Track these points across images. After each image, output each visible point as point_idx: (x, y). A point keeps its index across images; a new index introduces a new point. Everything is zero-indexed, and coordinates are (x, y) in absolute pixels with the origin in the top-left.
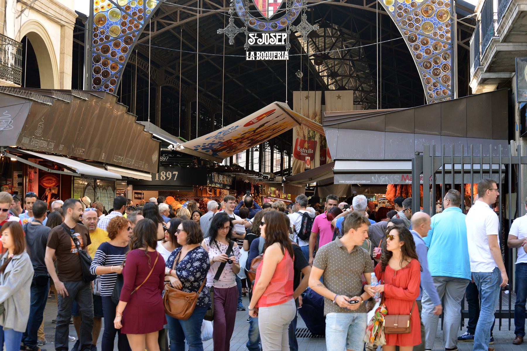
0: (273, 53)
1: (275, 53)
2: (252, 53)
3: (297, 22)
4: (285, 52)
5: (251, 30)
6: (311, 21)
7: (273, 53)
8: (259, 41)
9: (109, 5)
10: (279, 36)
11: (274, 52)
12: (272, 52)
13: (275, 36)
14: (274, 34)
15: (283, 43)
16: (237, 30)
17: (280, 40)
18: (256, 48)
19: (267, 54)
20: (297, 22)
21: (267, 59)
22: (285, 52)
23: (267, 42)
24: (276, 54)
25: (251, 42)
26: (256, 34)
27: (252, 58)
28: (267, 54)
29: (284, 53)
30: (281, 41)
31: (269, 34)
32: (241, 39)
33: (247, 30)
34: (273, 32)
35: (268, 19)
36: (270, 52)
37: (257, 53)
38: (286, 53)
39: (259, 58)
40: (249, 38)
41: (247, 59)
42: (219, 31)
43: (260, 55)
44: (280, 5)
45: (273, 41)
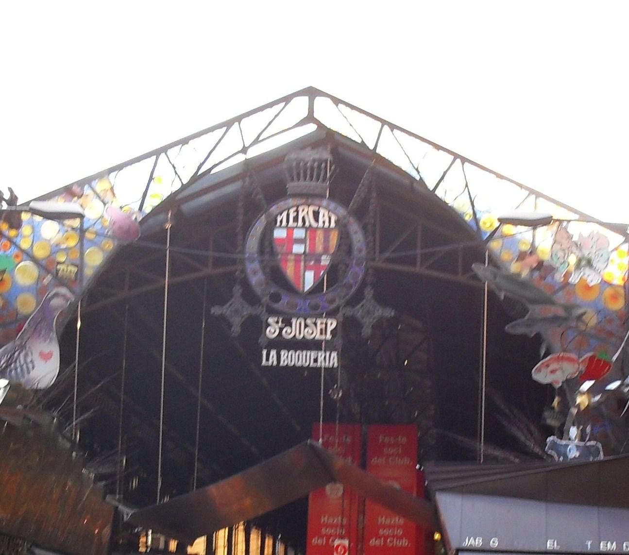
1: (313, 354)
3: (356, 299)
5: (272, 312)
6: (381, 299)
9: (17, 256)
13: (315, 324)
15: (329, 336)
16: (247, 310)
18: (280, 344)
20: (356, 299)
21: (299, 364)
23: (300, 333)
25: (272, 332)
31: (305, 320)
32: (256, 326)
33: (265, 311)
34: (311, 316)
38: (334, 354)
40: (268, 325)
41: (264, 362)
42: (216, 310)
43: (287, 357)
44: (325, 269)
45: (310, 332)
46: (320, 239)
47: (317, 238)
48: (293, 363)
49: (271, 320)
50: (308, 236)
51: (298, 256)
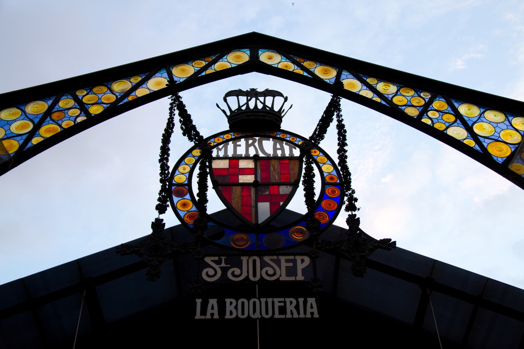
0: (273, 302)
1: (277, 302)
2: (213, 302)
4: (308, 299)
7: (273, 302)
8: (233, 274)
10: (287, 261)
11: (276, 300)
12: (270, 300)
14: (275, 257)
17: (292, 271)
19: (254, 303)
21: (257, 315)
22: (308, 299)
23: (255, 275)
24: (282, 304)
26: (223, 258)
27: (212, 315)
28: (254, 303)
29: (305, 303)
30: (296, 275)
31: (261, 255)
35: (257, 224)
36: (263, 300)
37: (228, 301)
38: (311, 301)
39: (231, 313)
41: (198, 316)
43: (236, 307)
45: (271, 272)
46: (276, 168)
47: (272, 169)
48: (246, 315)
49: (208, 260)
50: (258, 167)
51: (245, 185)
